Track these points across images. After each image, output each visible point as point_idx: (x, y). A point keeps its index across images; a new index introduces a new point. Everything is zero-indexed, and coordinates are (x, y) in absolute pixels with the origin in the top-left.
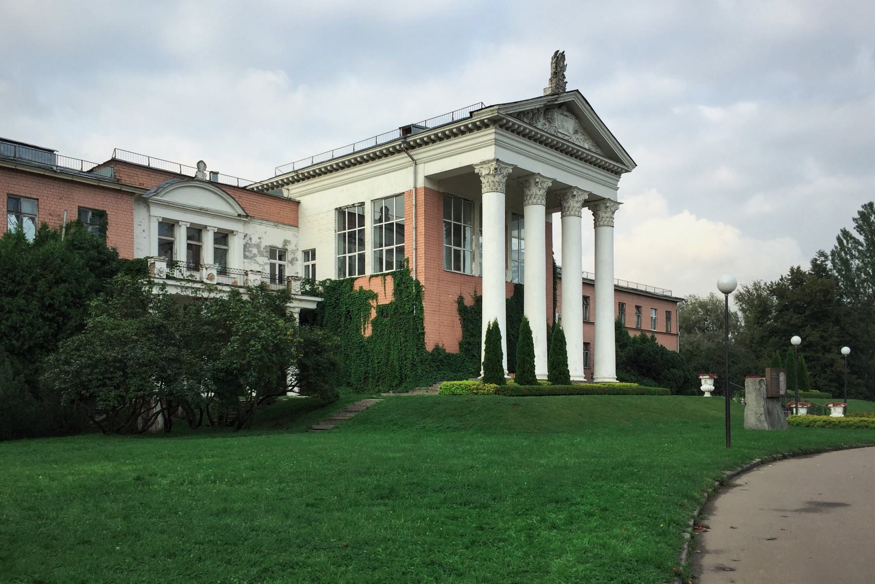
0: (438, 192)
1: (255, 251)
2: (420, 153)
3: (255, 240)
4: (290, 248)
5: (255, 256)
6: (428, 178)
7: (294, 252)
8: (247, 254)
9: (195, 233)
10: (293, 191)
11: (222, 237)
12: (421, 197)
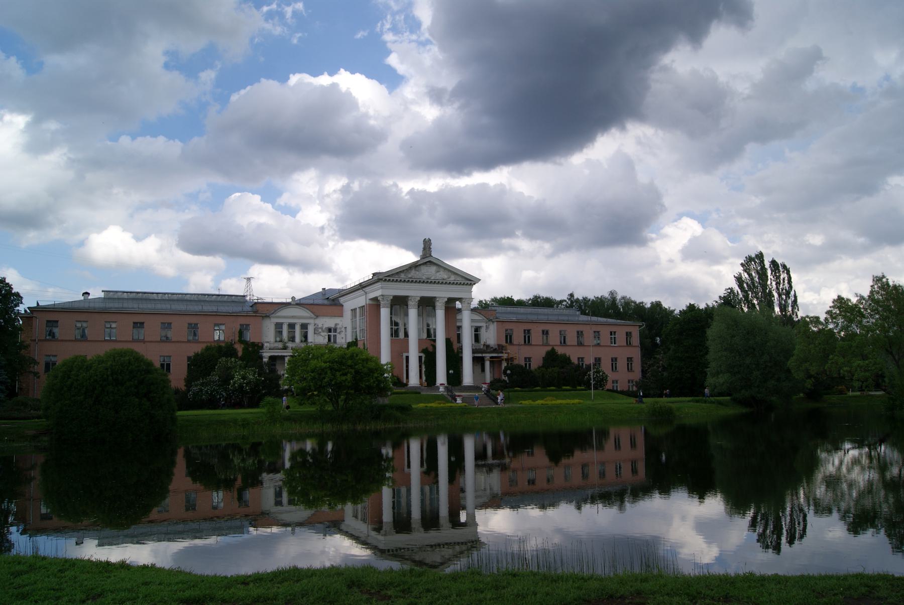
1: (320, 330)
2: (367, 289)
3: (320, 326)
4: (338, 327)
5: (320, 332)
6: (371, 299)
7: (340, 328)
8: (316, 332)
9: (292, 326)
10: (342, 300)
11: (304, 327)
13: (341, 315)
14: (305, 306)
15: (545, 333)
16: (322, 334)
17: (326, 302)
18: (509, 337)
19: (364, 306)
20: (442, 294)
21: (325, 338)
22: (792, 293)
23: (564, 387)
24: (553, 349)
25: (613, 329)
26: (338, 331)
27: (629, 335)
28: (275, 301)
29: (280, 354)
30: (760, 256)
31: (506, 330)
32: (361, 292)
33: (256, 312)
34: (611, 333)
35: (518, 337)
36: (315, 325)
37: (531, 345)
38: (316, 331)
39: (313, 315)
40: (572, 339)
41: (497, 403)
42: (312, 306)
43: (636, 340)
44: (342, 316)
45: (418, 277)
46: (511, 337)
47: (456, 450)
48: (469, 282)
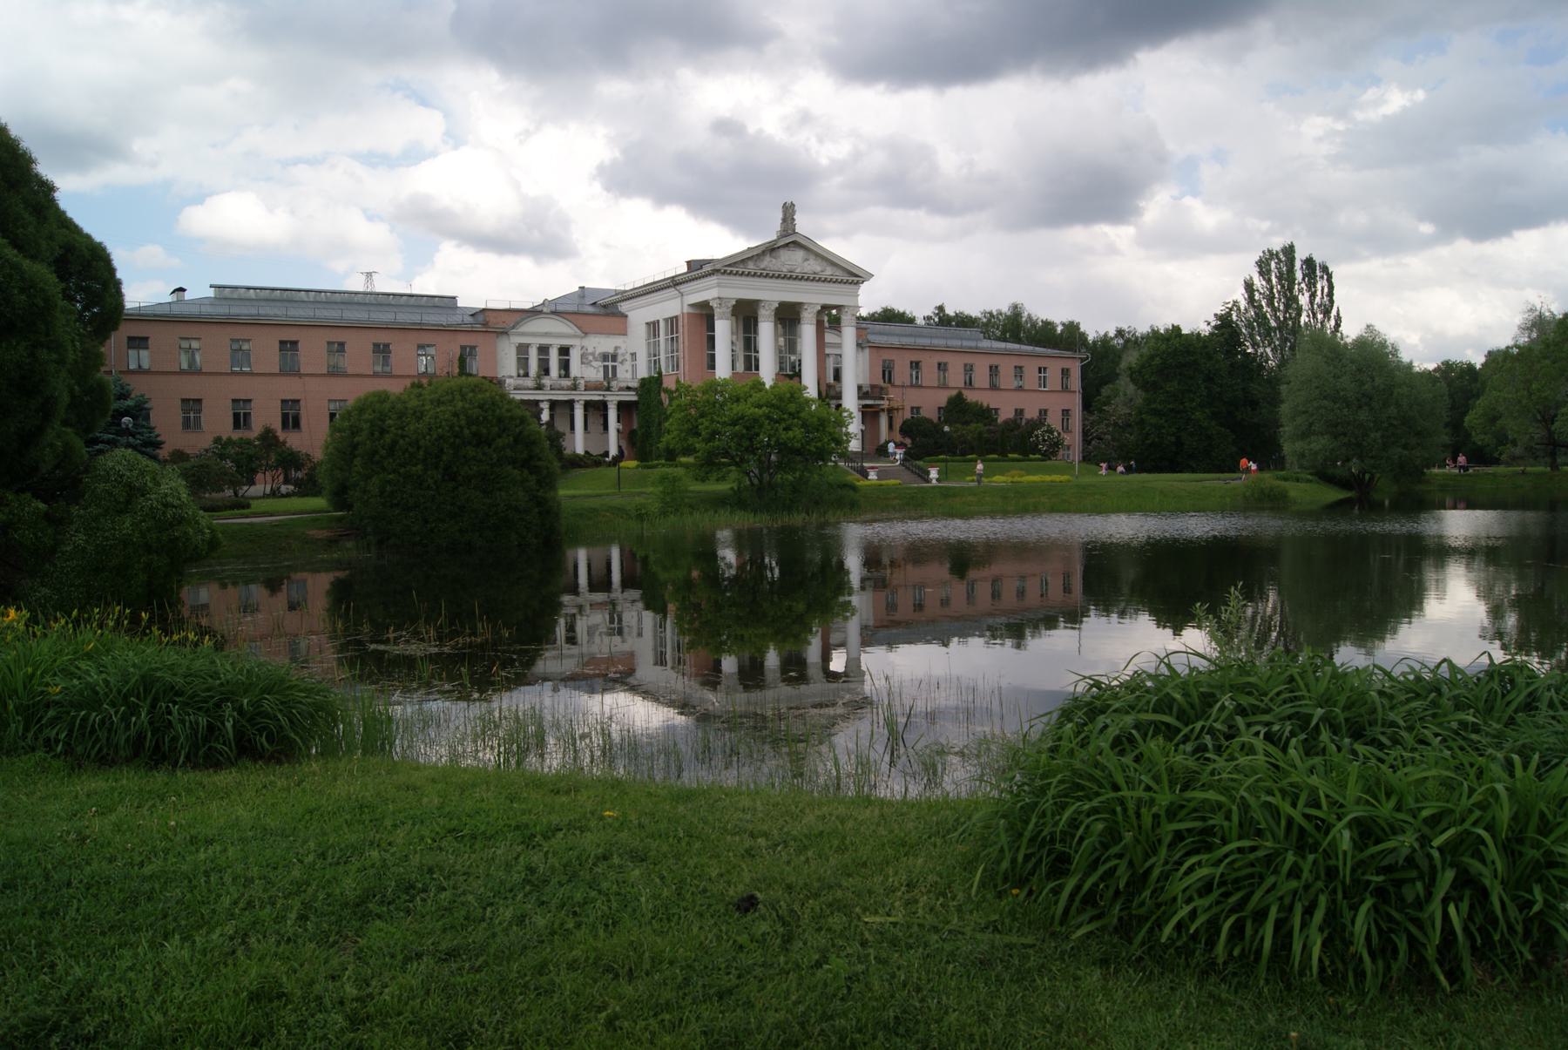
0: (701, 315)
1: (591, 358)
2: (683, 288)
3: (590, 350)
4: (620, 352)
7: (623, 355)
9: (543, 350)
10: (624, 307)
11: (564, 351)
12: (686, 321)
13: (624, 333)
14: (567, 316)
15: (942, 367)
16: (594, 364)
17: (591, 309)
18: (887, 373)
19: (676, 317)
20: (812, 297)
21: (598, 371)
22: (1334, 312)
23: (1010, 455)
24: (960, 395)
25: (1043, 363)
26: (620, 359)
27: (1065, 373)
28: (514, 306)
29: (532, 398)
30: (1289, 251)
31: (884, 361)
32: (672, 292)
33: (485, 324)
34: (1040, 369)
35: (902, 373)
36: (582, 348)
37: (921, 387)
38: (584, 359)
39: (579, 332)
40: (981, 377)
41: (928, 481)
42: (577, 317)
43: (1076, 382)
44: (625, 334)
46: (890, 373)
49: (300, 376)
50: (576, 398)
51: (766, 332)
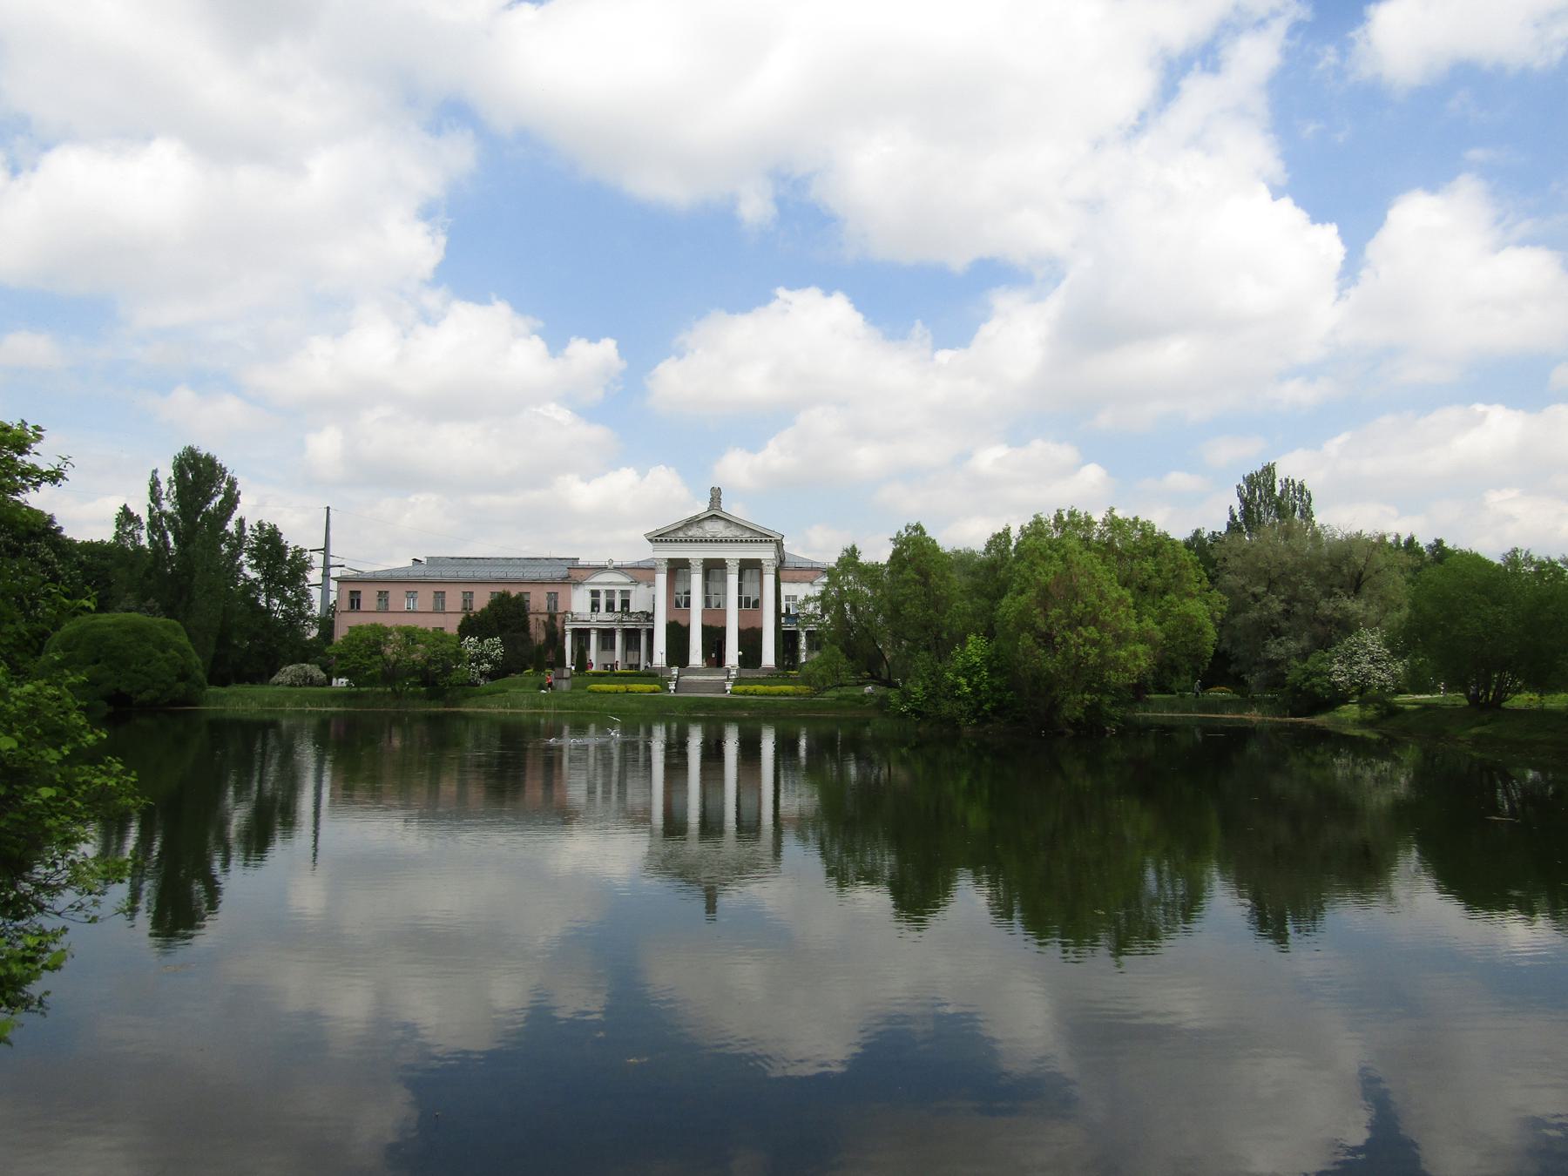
9: (610, 593)
14: (624, 571)
20: (733, 555)
45: (701, 535)
47: (750, 751)
48: (768, 539)
49: (445, 613)
50: (615, 627)
51: (697, 580)
